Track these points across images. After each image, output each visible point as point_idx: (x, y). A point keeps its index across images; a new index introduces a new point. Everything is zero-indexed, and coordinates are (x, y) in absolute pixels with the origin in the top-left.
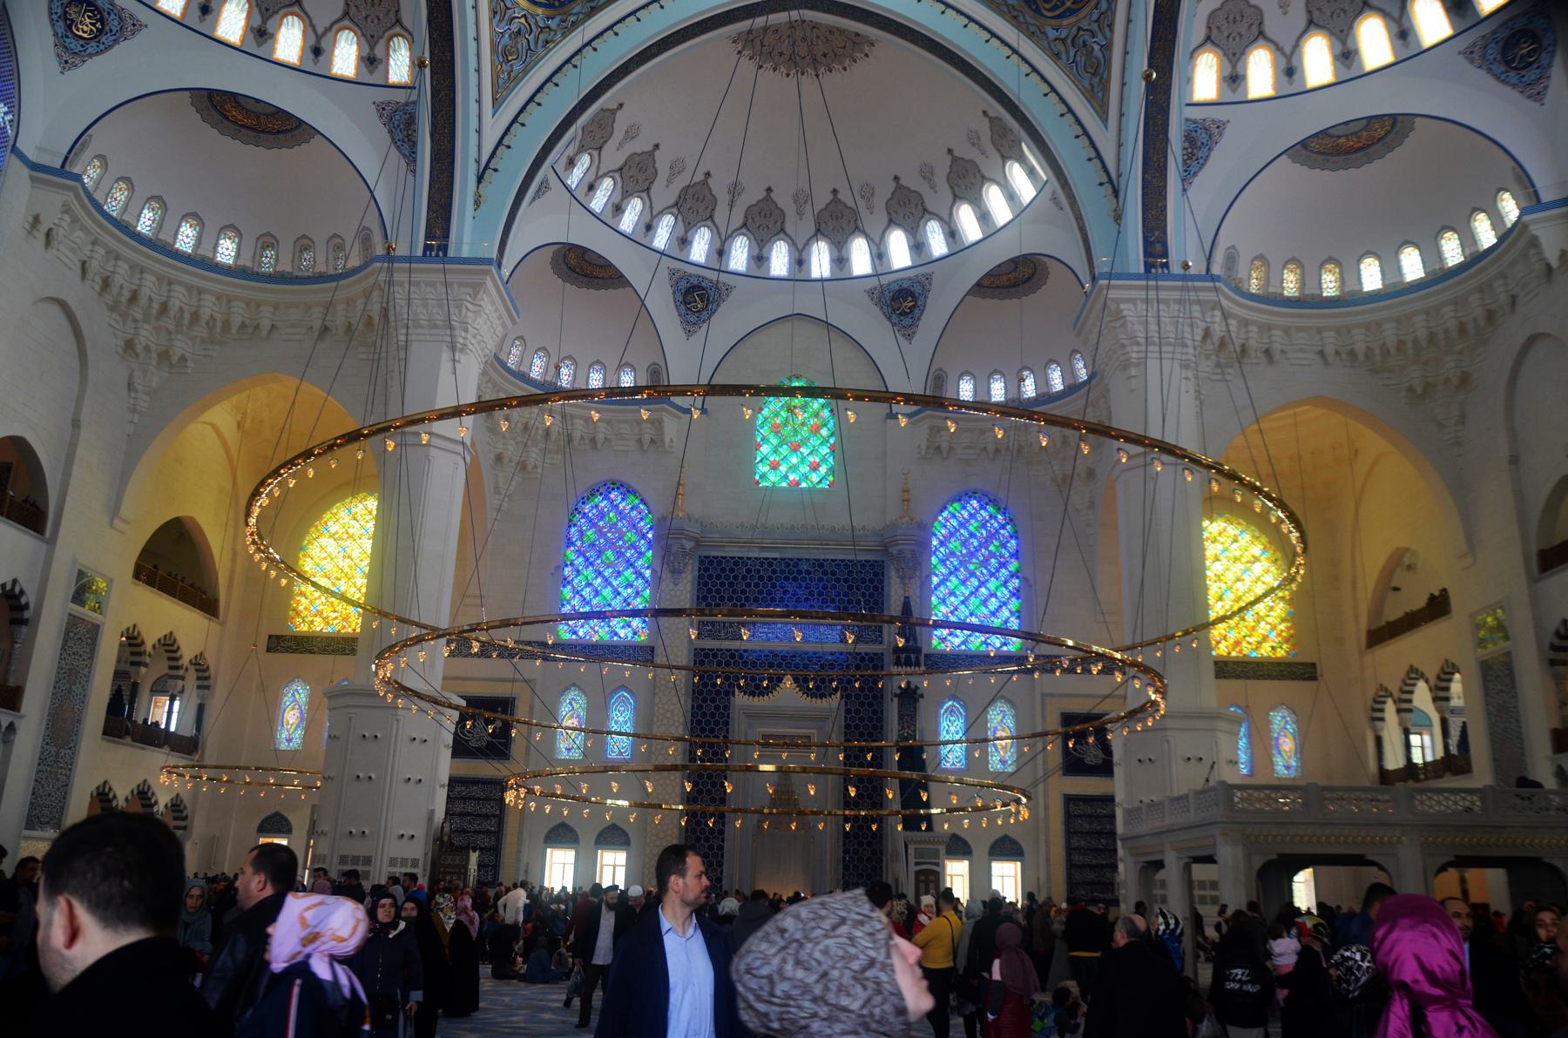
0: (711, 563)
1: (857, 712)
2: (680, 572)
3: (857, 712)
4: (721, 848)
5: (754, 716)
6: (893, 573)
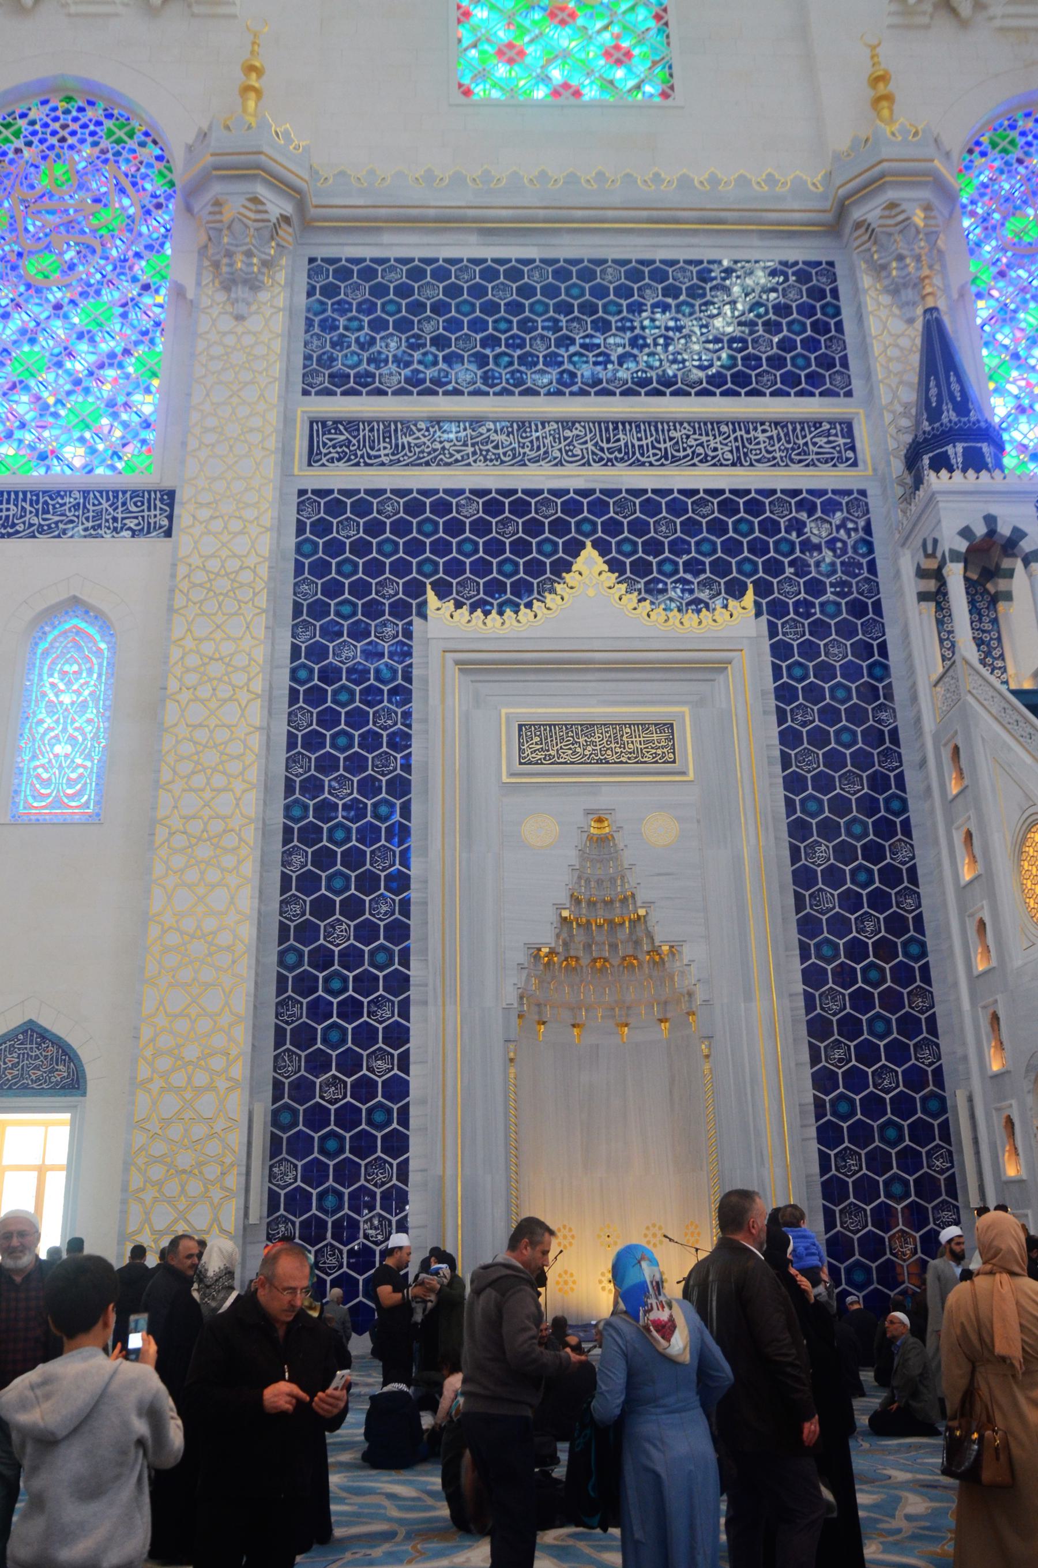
0: (343, 274)
1: (809, 650)
2: (253, 285)
3: (809, 650)
4: (398, 1089)
5: (477, 667)
6: (866, 281)
